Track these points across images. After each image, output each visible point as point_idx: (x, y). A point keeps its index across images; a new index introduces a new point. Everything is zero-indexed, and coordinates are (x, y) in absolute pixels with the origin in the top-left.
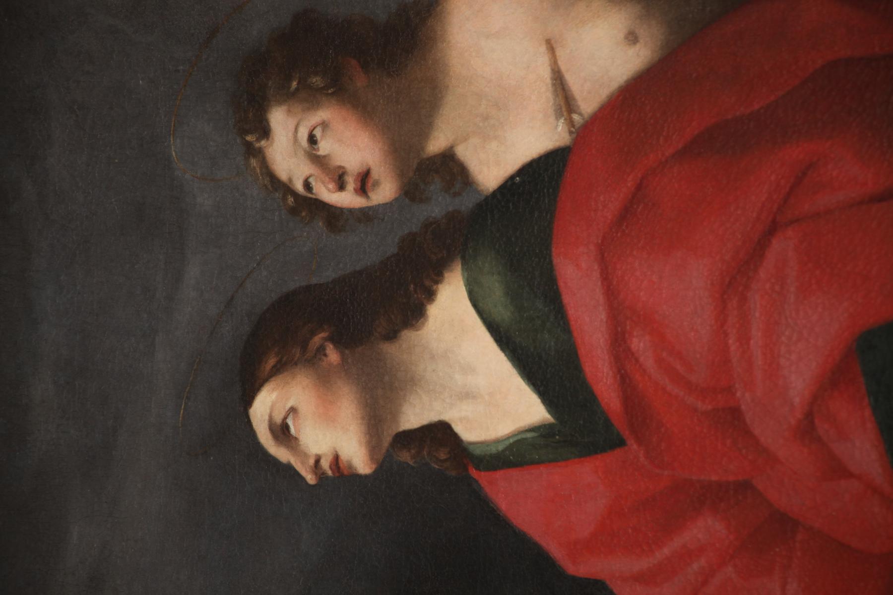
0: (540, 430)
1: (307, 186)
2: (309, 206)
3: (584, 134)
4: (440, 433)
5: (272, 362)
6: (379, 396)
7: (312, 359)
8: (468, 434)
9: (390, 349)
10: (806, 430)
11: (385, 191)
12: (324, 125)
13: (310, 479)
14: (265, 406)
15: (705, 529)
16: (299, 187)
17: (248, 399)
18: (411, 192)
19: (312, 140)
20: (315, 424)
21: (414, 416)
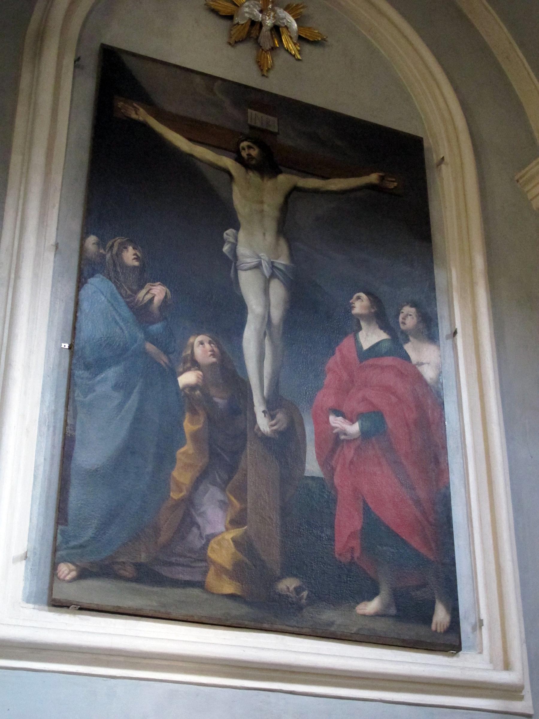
0: (361, 347)
1: (403, 312)
3: (414, 367)
4: (360, 328)
5: (371, 299)
6: (368, 318)
7: (372, 307)
8: (360, 334)
10: (364, 399)
12: (413, 318)
13: (350, 301)
15: (345, 377)
16: (402, 311)
17: (364, 293)
18: (403, 332)
19: (411, 315)
20: (360, 305)
21: (363, 324)
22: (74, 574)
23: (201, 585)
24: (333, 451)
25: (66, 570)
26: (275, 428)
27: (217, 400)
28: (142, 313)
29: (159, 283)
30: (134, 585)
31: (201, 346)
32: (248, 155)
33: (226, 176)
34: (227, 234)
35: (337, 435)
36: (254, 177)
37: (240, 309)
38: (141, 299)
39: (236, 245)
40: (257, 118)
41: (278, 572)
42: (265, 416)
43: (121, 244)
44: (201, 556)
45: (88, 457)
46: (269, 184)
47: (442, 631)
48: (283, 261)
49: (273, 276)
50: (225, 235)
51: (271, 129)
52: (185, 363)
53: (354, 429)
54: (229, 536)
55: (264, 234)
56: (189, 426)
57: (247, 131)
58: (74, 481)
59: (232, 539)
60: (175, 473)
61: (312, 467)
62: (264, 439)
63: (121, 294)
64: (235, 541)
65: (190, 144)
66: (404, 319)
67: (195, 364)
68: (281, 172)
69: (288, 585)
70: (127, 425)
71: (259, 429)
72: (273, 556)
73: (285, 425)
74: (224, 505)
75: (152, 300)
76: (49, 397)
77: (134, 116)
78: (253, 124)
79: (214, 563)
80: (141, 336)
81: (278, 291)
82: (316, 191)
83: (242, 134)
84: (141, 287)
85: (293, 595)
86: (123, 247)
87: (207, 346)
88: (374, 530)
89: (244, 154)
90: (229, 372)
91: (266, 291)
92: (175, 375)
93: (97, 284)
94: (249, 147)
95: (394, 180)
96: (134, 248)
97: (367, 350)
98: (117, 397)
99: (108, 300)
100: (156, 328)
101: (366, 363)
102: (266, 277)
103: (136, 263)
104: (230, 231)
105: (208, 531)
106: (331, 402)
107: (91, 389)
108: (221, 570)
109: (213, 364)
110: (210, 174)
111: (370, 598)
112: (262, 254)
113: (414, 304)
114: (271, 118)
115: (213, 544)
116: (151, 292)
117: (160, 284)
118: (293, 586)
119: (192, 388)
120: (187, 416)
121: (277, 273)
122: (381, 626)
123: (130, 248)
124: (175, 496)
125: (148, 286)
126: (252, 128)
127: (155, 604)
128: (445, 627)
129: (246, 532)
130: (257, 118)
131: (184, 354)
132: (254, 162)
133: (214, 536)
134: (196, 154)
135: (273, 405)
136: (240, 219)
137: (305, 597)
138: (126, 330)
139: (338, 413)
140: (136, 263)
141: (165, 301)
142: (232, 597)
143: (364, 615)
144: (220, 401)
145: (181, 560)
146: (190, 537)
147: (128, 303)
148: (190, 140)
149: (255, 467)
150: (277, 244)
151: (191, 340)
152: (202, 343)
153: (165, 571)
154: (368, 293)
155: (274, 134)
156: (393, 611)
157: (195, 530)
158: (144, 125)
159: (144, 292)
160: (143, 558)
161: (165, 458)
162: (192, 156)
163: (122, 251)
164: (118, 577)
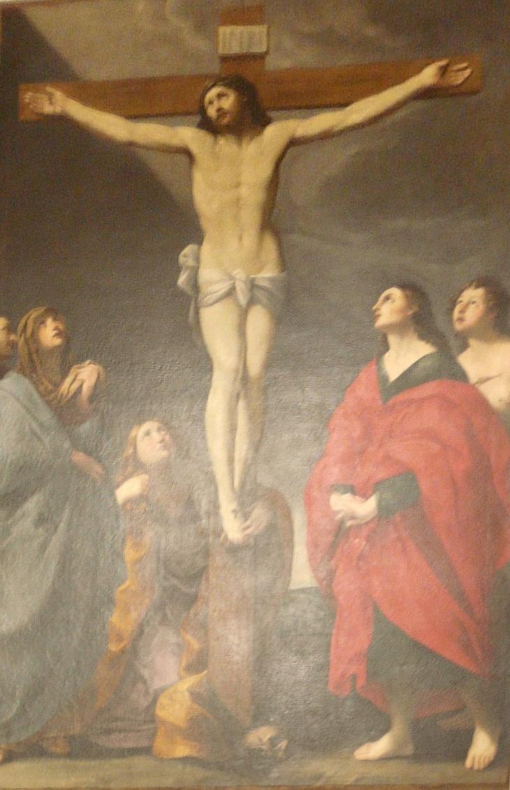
1: (461, 301)
2: (454, 303)
4: (386, 347)
6: (399, 328)
7: (409, 306)
9: (412, 328)
11: (458, 327)
13: (374, 308)
14: (396, 292)
16: (460, 299)
19: (474, 302)
20: (391, 307)
21: (393, 339)
23: (147, 751)
26: (249, 531)
29: (88, 362)
30: (68, 762)
31: (146, 438)
32: (219, 110)
33: (183, 159)
34: (185, 256)
35: (342, 522)
36: (226, 145)
38: (66, 392)
39: (198, 268)
42: (235, 517)
43: (36, 319)
47: (482, 767)
48: (268, 273)
49: (252, 302)
50: (181, 259)
52: (125, 467)
53: (366, 508)
55: (240, 238)
57: (215, 68)
59: (188, 690)
65: (131, 125)
66: (462, 312)
67: (138, 466)
68: (267, 122)
71: (226, 538)
75: (81, 386)
77: (48, 109)
79: (163, 722)
80: (67, 445)
81: (259, 322)
82: (326, 136)
83: (207, 76)
84: (65, 374)
86: (41, 322)
87: (156, 436)
89: (212, 112)
94: (220, 96)
95: (464, 65)
96: (55, 319)
97: (393, 382)
99: (22, 404)
102: (241, 306)
103: (58, 341)
104: (189, 250)
108: (174, 730)
110: (158, 164)
111: (375, 739)
112: (237, 271)
113: (480, 282)
115: (163, 700)
116: (80, 377)
117: (90, 363)
118: (268, 737)
121: (259, 294)
124: (114, 647)
126: (225, 59)
127: (93, 780)
128: (487, 760)
132: (225, 121)
133: (163, 690)
135: (247, 496)
136: (204, 223)
137: (283, 748)
140: (58, 341)
142: (185, 760)
143: (366, 761)
146: (134, 696)
147: (48, 403)
151: (133, 433)
152: (148, 433)
153: (104, 741)
154: (403, 286)
155: (261, 57)
157: (140, 686)
158: (63, 120)
159: (69, 380)
160: (77, 729)
162: (131, 144)
163: (39, 328)
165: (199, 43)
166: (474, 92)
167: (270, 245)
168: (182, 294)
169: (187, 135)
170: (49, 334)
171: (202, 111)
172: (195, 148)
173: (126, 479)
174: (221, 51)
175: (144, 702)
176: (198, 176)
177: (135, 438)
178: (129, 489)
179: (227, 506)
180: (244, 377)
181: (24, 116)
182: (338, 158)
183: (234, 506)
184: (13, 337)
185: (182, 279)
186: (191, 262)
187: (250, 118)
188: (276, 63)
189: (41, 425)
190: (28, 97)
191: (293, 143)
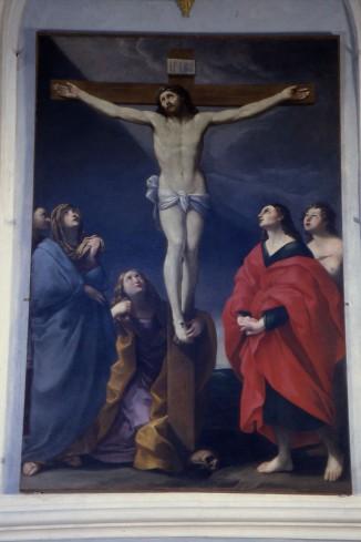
2: (304, 215)
3: (317, 262)
6: (274, 227)
7: (279, 216)
10: (270, 298)
11: (307, 228)
14: (271, 208)
15: (253, 281)
20: (268, 216)
21: (270, 233)
22: (35, 469)
23: (130, 465)
24: (239, 347)
25: (30, 468)
27: (142, 321)
28: (81, 263)
32: (169, 104)
35: (245, 331)
36: (173, 123)
37: (162, 242)
40: (176, 65)
41: (192, 448)
44: (131, 443)
45: (45, 383)
46: (187, 126)
48: (198, 193)
49: (190, 208)
50: (148, 183)
51: (189, 73)
53: (260, 324)
54: (153, 425)
55: (182, 174)
56: (120, 346)
57: (166, 81)
58: (33, 404)
59: (157, 429)
60: (110, 384)
61: (222, 361)
62: (182, 346)
63: (64, 251)
64: (157, 429)
65: (116, 107)
66: (309, 220)
67: (124, 295)
68: (197, 112)
69: (201, 456)
70: (71, 355)
72: (188, 435)
73: (199, 332)
74: (149, 402)
75: (89, 251)
76: (15, 341)
77: (68, 94)
78: (172, 73)
80: (81, 282)
81: (194, 220)
82: (230, 122)
83: (161, 85)
84: (80, 242)
85: (205, 463)
86: (64, 212)
87: (134, 279)
88: (274, 401)
89: (164, 104)
90: (153, 297)
91: (184, 223)
92: (108, 307)
93: (46, 245)
94: (169, 96)
98: (65, 332)
100: (93, 273)
101: (273, 266)
102: (182, 210)
105: (136, 424)
106: (238, 307)
107: (44, 331)
108: (146, 451)
109: (139, 293)
110: (133, 130)
111: (269, 458)
113: (318, 205)
114: (189, 61)
115: (140, 433)
119: (122, 315)
120: (119, 338)
122: (279, 479)
123: (70, 212)
124: (110, 401)
125: (85, 240)
126: (171, 76)
129: (167, 423)
130: (176, 65)
131: (116, 289)
132: (172, 109)
133: (142, 426)
134: (122, 116)
135: (189, 316)
136: (161, 164)
138: (70, 279)
139: (245, 314)
140: (75, 224)
141: (99, 251)
142: (155, 471)
143: (265, 474)
144: (145, 322)
145: (116, 448)
147: (70, 258)
148: (116, 103)
149: (175, 371)
150: (193, 179)
151: (121, 277)
152: (130, 278)
153: (104, 458)
155: (192, 77)
156: (290, 467)
157: (125, 424)
158: (77, 101)
159: (82, 245)
160: (86, 451)
161: (102, 372)
164: (72, 467)
165: (157, 67)
166: (312, 104)
167: (199, 179)
168: (149, 201)
169: (150, 116)
170: (70, 219)
171: (159, 104)
172: (154, 124)
173: (117, 302)
174: (169, 72)
175: (130, 434)
176: (157, 139)
177: (122, 281)
178: (119, 308)
179: (177, 321)
180: (185, 249)
181: (54, 97)
182: (237, 134)
183: (180, 321)
184: (48, 219)
185: (149, 194)
186: (154, 185)
187: (185, 110)
188: (201, 81)
189: (66, 270)
190: (56, 87)
191: (212, 124)
